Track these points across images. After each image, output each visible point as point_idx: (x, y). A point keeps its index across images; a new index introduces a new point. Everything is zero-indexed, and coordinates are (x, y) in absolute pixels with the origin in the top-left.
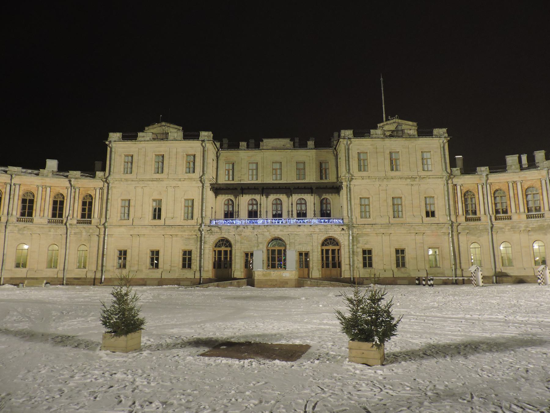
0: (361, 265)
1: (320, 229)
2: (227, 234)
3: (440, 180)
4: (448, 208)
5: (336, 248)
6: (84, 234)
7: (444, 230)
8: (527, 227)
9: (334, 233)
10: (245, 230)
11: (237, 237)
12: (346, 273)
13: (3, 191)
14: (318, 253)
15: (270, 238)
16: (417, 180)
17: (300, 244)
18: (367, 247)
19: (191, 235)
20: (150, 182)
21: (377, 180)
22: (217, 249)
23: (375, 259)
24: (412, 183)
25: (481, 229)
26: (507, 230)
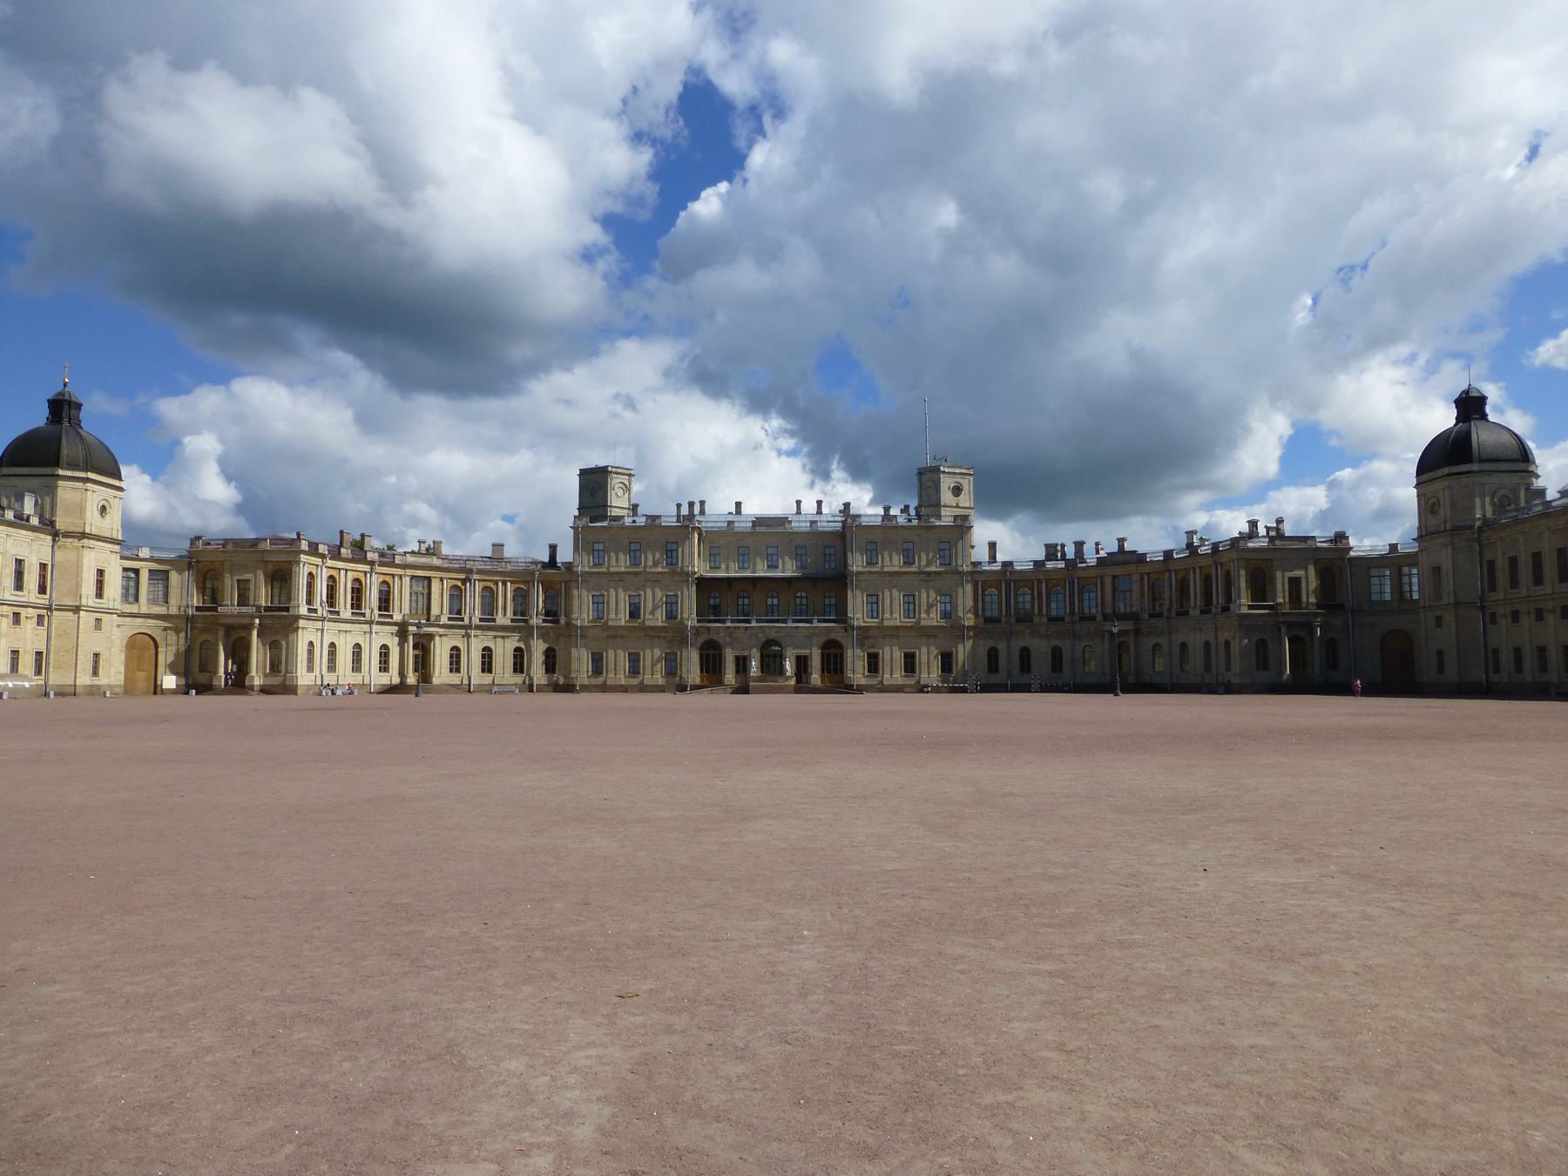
5: (839, 651)
10: (737, 631)
11: (728, 639)
13: (463, 588)
15: (764, 640)
16: (933, 575)
19: (676, 636)
22: (704, 652)
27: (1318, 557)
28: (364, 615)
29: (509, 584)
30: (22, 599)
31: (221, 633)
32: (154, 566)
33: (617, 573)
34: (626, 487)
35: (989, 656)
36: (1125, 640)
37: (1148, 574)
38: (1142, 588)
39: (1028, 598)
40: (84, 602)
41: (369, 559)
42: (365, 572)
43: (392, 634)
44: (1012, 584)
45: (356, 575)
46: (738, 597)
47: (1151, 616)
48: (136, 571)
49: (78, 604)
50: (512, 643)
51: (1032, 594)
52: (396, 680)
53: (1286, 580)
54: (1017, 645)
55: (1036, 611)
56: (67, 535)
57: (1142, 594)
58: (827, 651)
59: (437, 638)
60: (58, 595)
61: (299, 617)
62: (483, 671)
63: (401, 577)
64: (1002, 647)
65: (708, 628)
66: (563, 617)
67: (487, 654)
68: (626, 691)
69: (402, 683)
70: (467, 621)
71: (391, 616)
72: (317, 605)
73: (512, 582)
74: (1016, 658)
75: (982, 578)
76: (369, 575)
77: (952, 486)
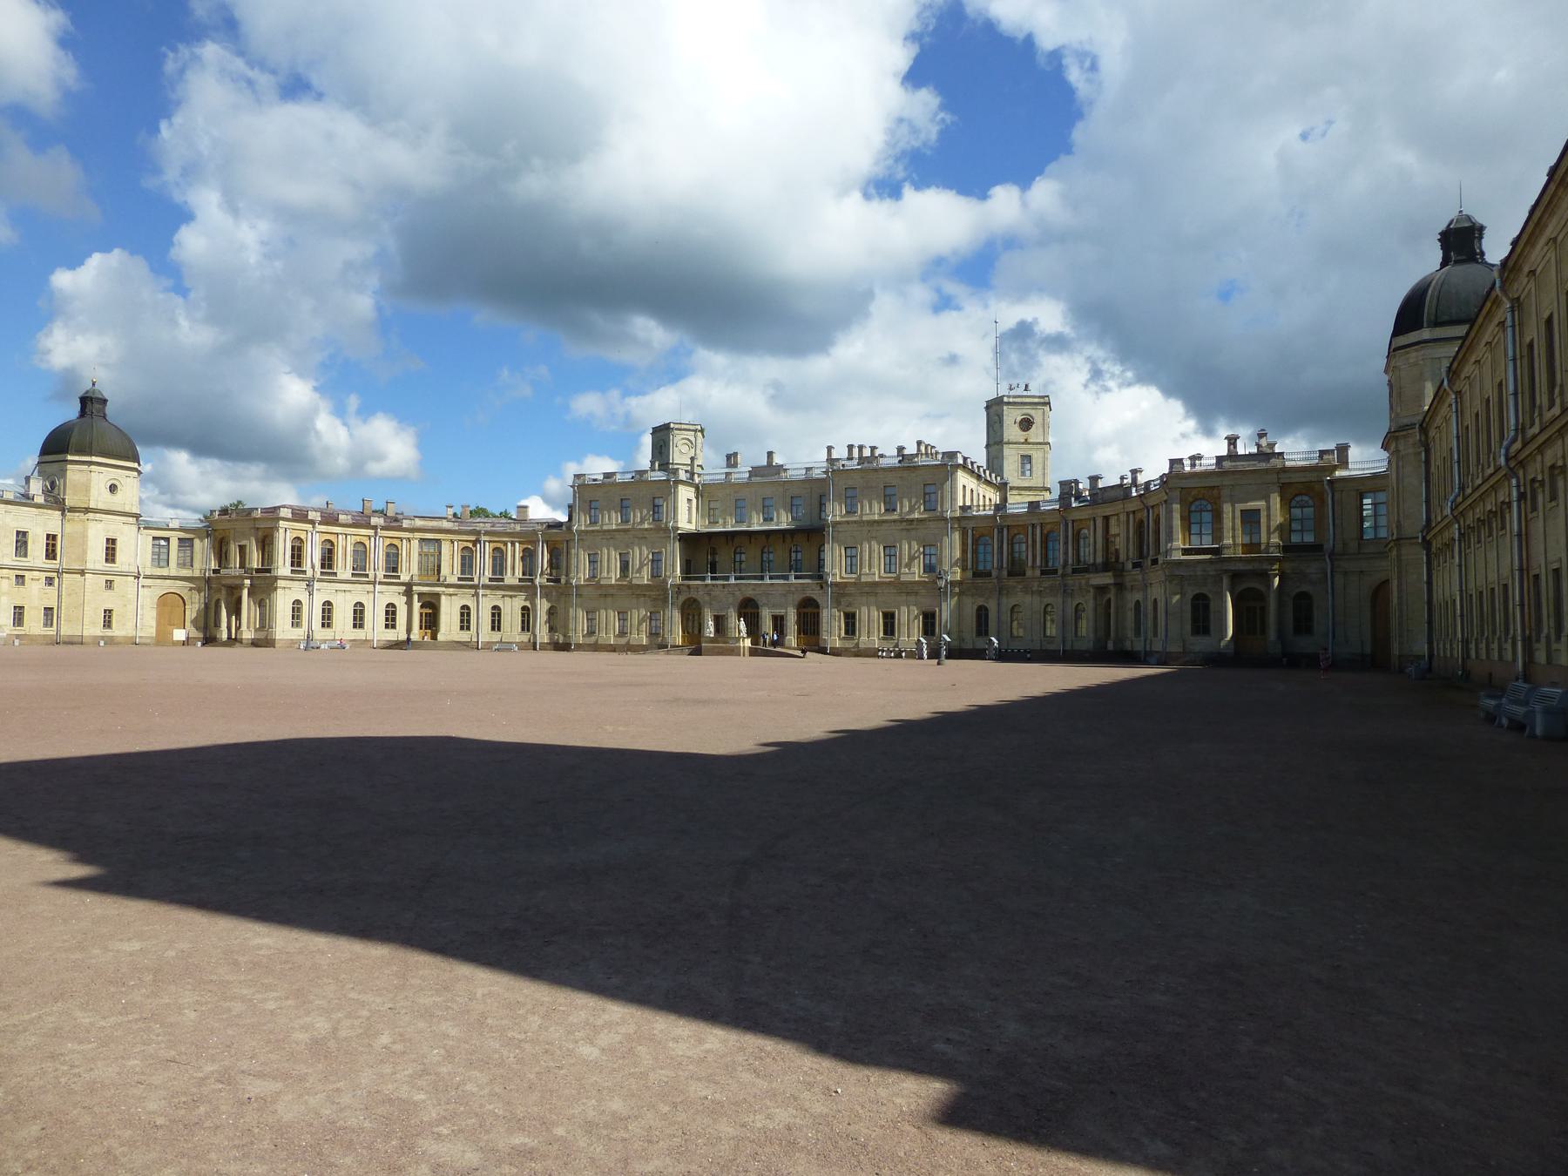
4: (958, 554)
5: (815, 611)
6: (554, 594)
11: (707, 598)
13: (474, 549)
15: (741, 598)
19: (659, 595)
24: (908, 527)
27: (1287, 481)
28: (367, 576)
29: (517, 545)
30: (27, 564)
31: (224, 592)
32: (182, 535)
33: (609, 531)
34: (692, 443)
35: (979, 616)
37: (1134, 512)
39: (1024, 546)
40: (90, 566)
41: (372, 524)
42: (369, 537)
43: (399, 593)
44: (1005, 530)
45: (358, 539)
46: (735, 553)
47: (1136, 565)
48: (167, 540)
49: (81, 568)
50: (519, 602)
52: (403, 637)
53: (1238, 514)
55: (1030, 564)
56: (73, 510)
58: (806, 610)
59: (443, 598)
60: (64, 559)
61: (276, 578)
62: (493, 629)
63: (409, 540)
64: (992, 606)
65: (688, 586)
66: (564, 577)
67: (496, 612)
68: (615, 651)
69: (409, 639)
70: (476, 582)
71: (399, 577)
72: (307, 566)
73: (520, 543)
75: (972, 524)
76: (373, 539)
77: (1019, 419)
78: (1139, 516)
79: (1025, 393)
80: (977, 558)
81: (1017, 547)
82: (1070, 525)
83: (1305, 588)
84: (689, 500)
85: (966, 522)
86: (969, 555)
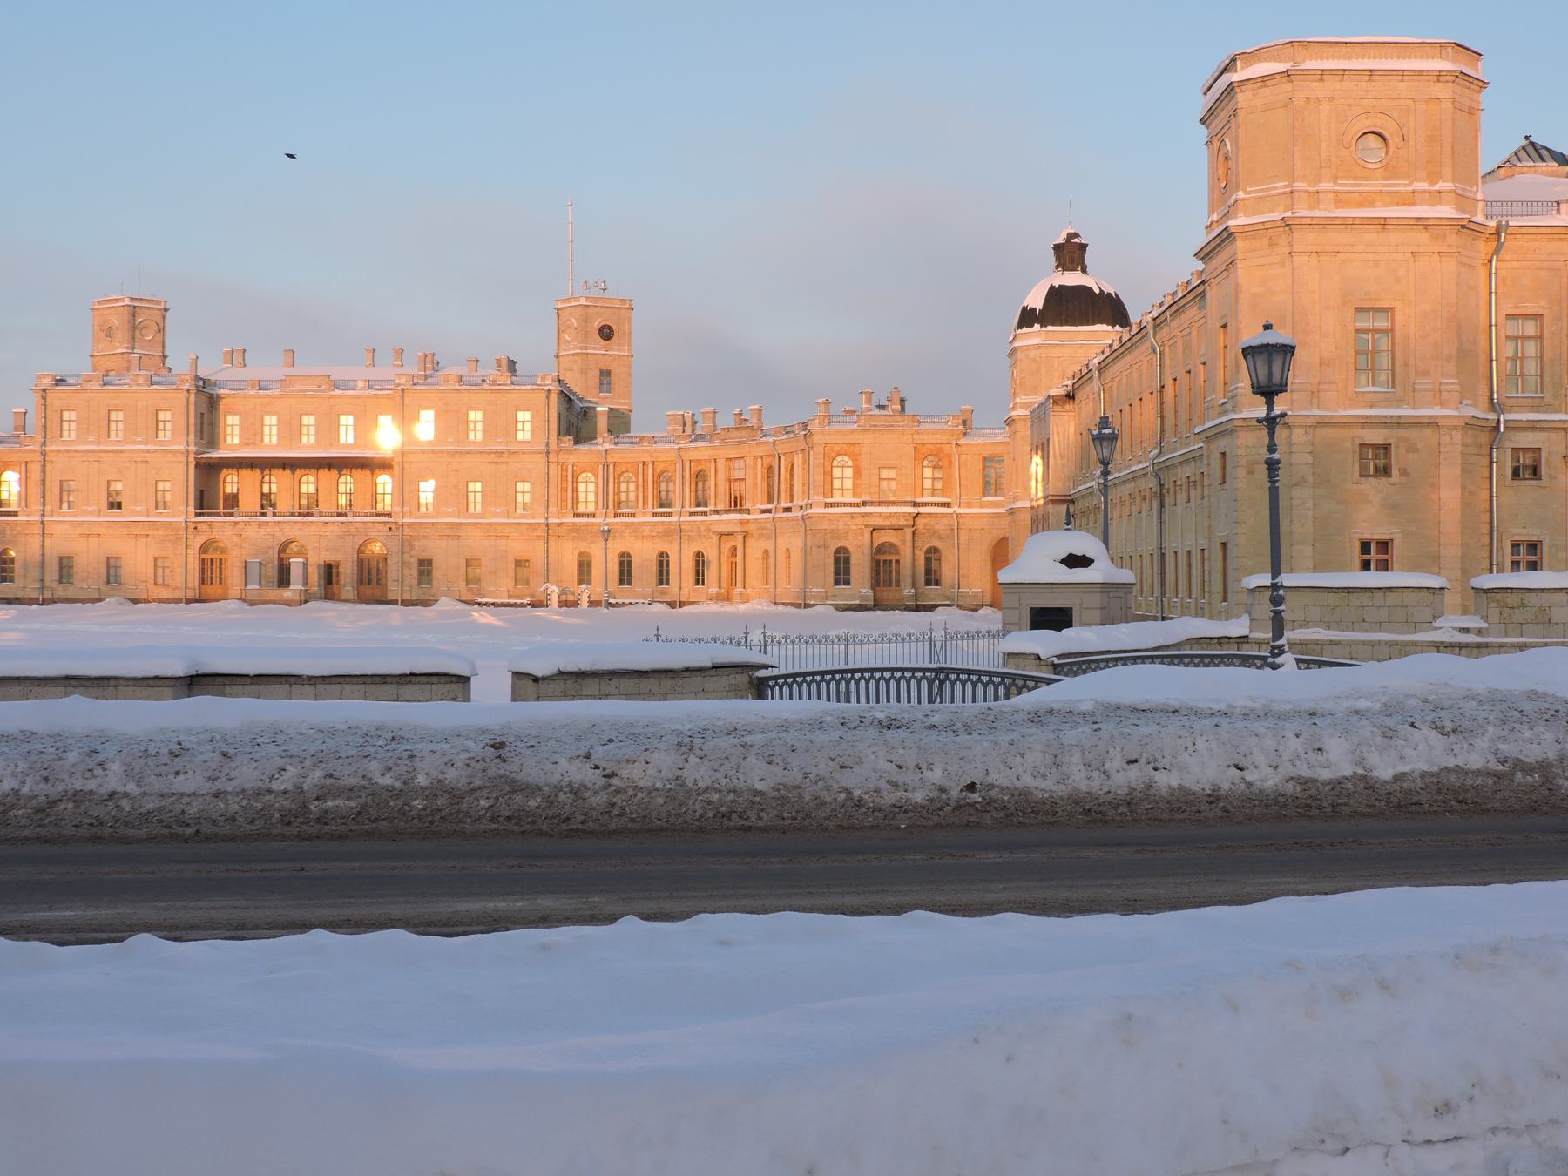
0: (415, 582)
1: (356, 528)
2: (220, 533)
3: (540, 455)
7: (539, 533)
8: (652, 531)
9: (377, 534)
10: (248, 528)
11: (236, 539)
12: (393, 591)
14: (353, 563)
16: (506, 455)
17: (327, 550)
18: (424, 556)
20: (104, 454)
21: (445, 455)
23: (436, 573)
24: (498, 460)
25: (594, 531)
26: (627, 534)
35: (581, 564)
36: (733, 544)
38: (755, 474)
39: (632, 486)
44: (611, 467)
51: (637, 482)
54: (616, 548)
57: (755, 484)
64: (596, 551)
65: (210, 524)
74: (614, 567)
78: (767, 461)
79: (601, 294)
80: (577, 499)
81: (623, 487)
82: (687, 464)
83: (936, 543)
84: (202, 414)
85: (566, 456)
86: (570, 494)
